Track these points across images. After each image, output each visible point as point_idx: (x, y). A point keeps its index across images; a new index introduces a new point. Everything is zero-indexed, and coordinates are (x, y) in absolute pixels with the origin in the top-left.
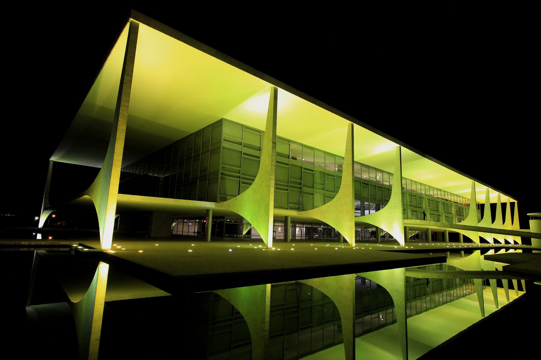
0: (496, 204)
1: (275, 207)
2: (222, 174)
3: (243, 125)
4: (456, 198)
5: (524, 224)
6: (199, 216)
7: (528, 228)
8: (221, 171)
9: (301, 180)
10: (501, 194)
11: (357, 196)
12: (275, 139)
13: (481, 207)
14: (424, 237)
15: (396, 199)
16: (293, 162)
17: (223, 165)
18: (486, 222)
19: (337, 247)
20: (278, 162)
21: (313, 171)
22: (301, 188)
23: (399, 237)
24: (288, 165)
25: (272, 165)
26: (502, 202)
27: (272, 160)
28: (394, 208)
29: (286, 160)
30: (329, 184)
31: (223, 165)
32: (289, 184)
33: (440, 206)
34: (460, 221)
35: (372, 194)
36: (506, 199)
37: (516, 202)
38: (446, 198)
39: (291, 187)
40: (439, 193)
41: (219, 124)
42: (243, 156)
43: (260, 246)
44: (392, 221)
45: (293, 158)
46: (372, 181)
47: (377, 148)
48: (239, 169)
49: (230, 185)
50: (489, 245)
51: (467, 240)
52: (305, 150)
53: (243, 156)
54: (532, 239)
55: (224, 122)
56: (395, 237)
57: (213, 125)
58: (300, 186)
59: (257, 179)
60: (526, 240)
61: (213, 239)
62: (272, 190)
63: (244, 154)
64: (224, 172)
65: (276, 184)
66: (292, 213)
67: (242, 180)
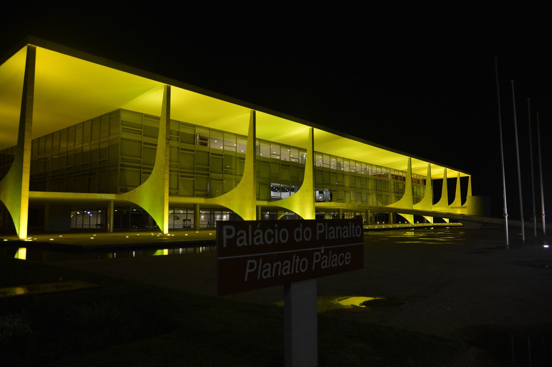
2: (122, 165)
8: (120, 162)
17: (122, 157)
22: (208, 175)
24: (193, 151)
31: (122, 157)
32: (195, 171)
39: (197, 173)
42: (143, 145)
48: (139, 159)
49: (130, 175)
52: (213, 133)
53: (143, 145)
58: (208, 173)
63: (145, 143)
64: (122, 163)
66: (200, 201)
67: (142, 170)
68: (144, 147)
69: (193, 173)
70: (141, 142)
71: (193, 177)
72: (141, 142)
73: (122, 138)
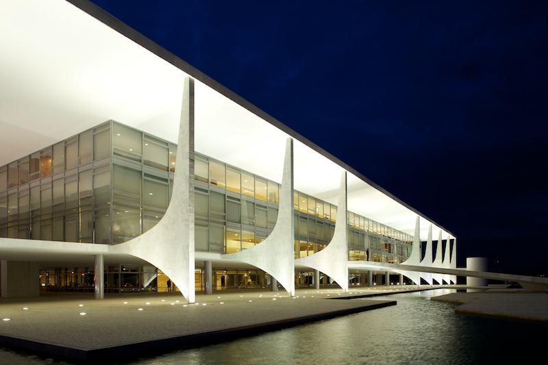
0: (437, 241)
1: (197, 250)
2: (114, 203)
3: (141, 133)
4: (362, 222)
5: (461, 263)
6: (85, 266)
7: (465, 266)
9: (223, 211)
10: (421, 217)
11: (352, 246)
12: (193, 156)
13: (423, 245)
14: (364, 281)
15: (340, 237)
16: (212, 188)
18: (427, 262)
19: (275, 296)
20: (196, 188)
21: (239, 200)
23: (342, 279)
24: (207, 191)
25: (190, 192)
26: (443, 239)
27: (190, 185)
28: (338, 247)
29: (137, 166)
30: (260, 220)
32: (211, 219)
33: (388, 247)
34: (402, 262)
35: (314, 231)
36: (447, 236)
37: (455, 238)
38: (389, 235)
39: (212, 221)
40: (383, 229)
41: (104, 129)
42: (144, 177)
43: (178, 302)
44: (334, 262)
45: (212, 183)
46: (310, 215)
47: (321, 174)
50: (428, 286)
51: (408, 281)
52: (229, 172)
54: (468, 277)
55: (112, 126)
56: (414, 280)
57: (94, 129)
58: (224, 221)
59: (169, 211)
60: (462, 280)
61: (321, 287)
62: (192, 225)
65: (196, 219)
68: (144, 180)
69: (208, 221)
70: (141, 172)
71: (207, 226)
72: (141, 172)
73: (114, 164)
